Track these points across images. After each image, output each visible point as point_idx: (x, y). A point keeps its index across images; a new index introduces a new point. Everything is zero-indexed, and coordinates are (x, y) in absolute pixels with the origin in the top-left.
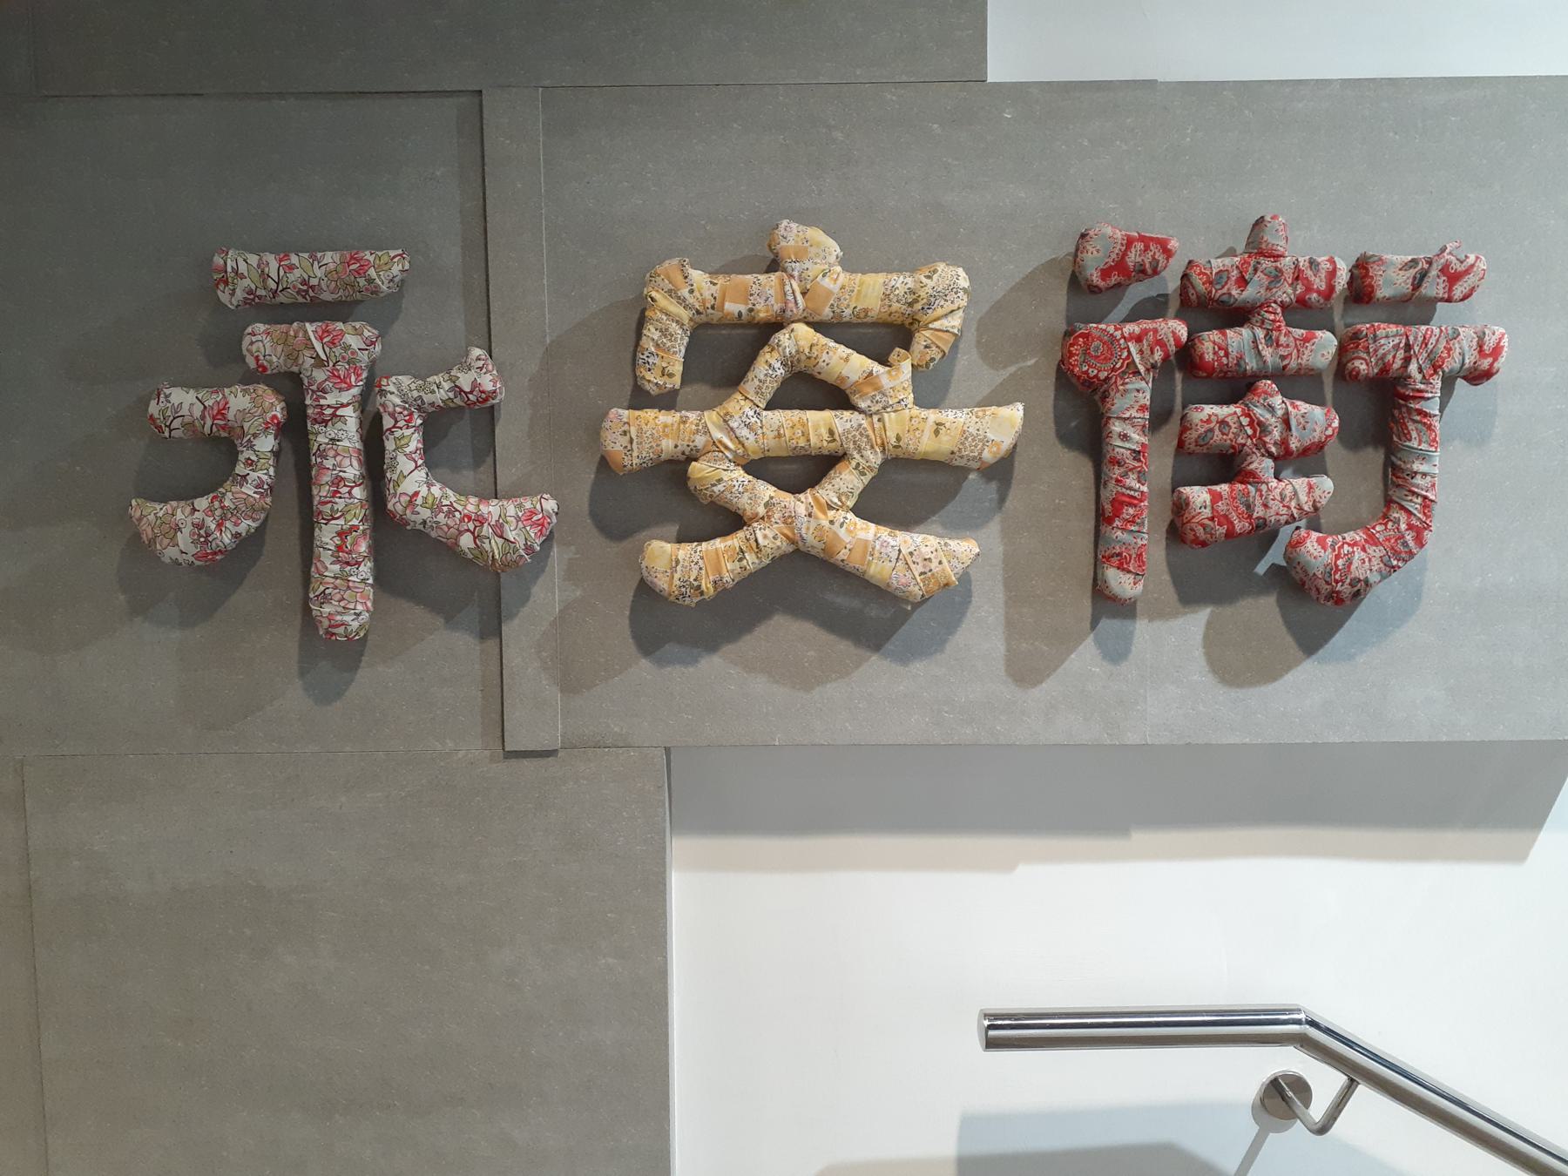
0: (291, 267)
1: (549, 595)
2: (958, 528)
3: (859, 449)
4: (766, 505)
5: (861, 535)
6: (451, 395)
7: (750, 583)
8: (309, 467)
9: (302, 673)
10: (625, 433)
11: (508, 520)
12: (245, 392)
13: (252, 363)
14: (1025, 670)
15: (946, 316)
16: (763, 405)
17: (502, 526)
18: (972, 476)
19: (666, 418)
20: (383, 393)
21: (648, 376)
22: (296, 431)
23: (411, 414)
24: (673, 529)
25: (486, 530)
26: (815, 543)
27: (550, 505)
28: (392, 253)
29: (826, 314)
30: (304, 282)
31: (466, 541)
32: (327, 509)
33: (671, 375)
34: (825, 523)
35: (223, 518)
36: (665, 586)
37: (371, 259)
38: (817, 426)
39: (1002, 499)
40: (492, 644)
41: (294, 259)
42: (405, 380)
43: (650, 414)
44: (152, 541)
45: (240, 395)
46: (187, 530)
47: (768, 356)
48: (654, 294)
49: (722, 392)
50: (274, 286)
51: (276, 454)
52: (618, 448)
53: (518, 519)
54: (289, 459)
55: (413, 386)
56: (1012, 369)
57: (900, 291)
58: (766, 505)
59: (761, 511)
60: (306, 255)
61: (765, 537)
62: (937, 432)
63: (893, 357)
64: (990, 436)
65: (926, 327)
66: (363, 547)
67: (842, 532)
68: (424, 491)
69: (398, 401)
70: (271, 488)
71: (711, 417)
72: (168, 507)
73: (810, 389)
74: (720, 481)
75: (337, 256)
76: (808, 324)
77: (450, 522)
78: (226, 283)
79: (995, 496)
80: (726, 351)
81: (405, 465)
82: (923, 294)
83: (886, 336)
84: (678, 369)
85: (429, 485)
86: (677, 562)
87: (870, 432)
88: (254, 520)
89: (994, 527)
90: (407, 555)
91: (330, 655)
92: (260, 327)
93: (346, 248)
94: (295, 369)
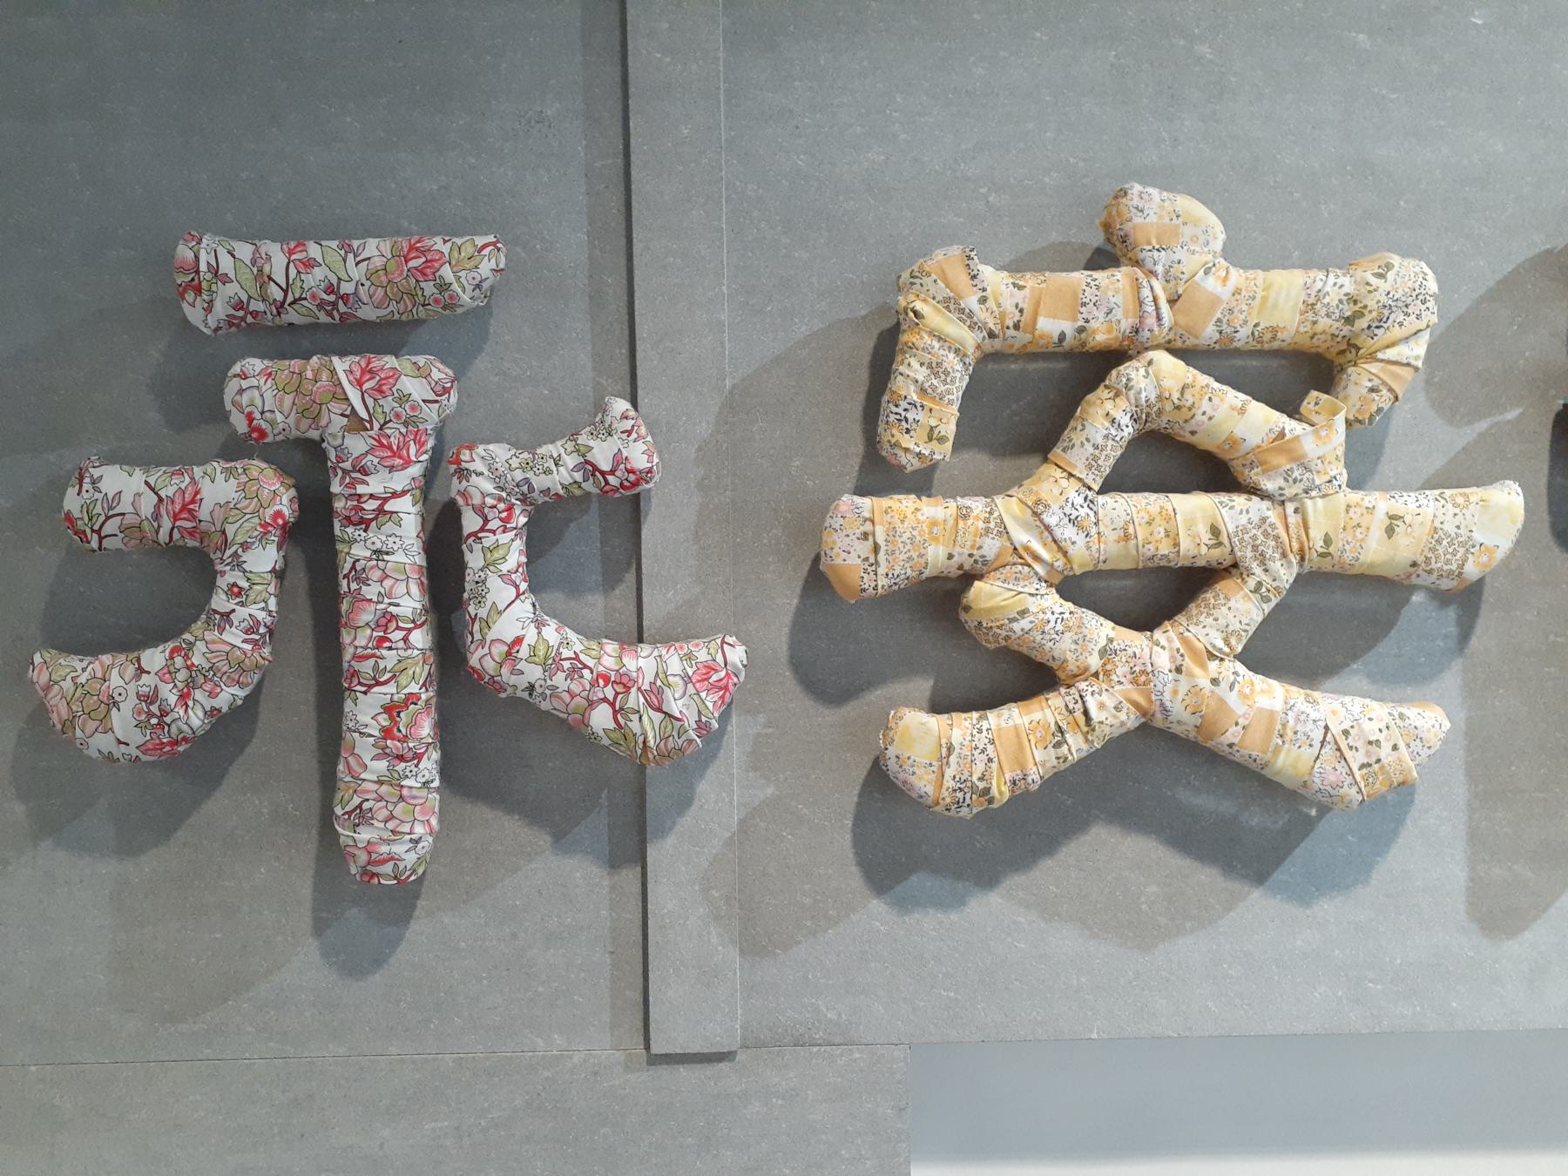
0: (310, 264)
1: (723, 796)
2: (1401, 680)
3: (1262, 560)
4: (1103, 652)
5: (1263, 702)
6: (578, 476)
7: (1062, 780)
8: (337, 597)
9: (319, 927)
10: (865, 536)
11: (670, 679)
12: (229, 473)
13: (240, 425)
14: (1497, 913)
15: (1406, 339)
16: (1096, 488)
17: (660, 692)
18: (1417, 598)
19: (934, 510)
20: (463, 474)
21: (906, 441)
22: (313, 535)
23: (510, 509)
24: (923, 686)
25: (635, 700)
26: (1185, 715)
27: (737, 655)
28: (480, 241)
29: (1208, 334)
30: (330, 289)
31: (601, 719)
32: (366, 667)
33: (942, 440)
34: (1204, 683)
35: (191, 684)
36: (930, 790)
37: (446, 249)
38: (1189, 520)
39: (1465, 636)
40: (630, 875)
41: (314, 251)
42: (501, 452)
43: (905, 503)
44: (69, 724)
45: (220, 478)
46: (129, 705)
47: (1109, 405)
48: (919, 306)
49: (1010, 465)
50: (279, 295)
51: (279, 575)
52: (853, 560)
53: (687, 679)
54: (299, 578)
55: (515, 463)
56: (1482, 426)
57: (1333, 297)
58: (1103, 652)
59: (1094, 662)
60: (334, 244)
61: (1102, 706)
62: (1390, 531)
63: (1307, 406)
64: (1478, 537)
65: (1372, 357)
66: (426, 729)
67: (1232, 699)
68: (531, 635)
69: (488, 487)
70: (271, 632)
71: (1009, 507)
72: (96, 666)
73: (1175, 458)
74: (1023, 613)
75: (386, 246)
76: (1175, 352)
77: (575, 687)
78: (198, 290)
79: (1453, 630)
80: (1032, 402)
81: (500, 592)
82: (1372, 304)
83: (1299, 372)
84: (949, 429)
85: (539, 625)
86: (950, 749)
87: (1281, 531)
88: (242, 686)
89: (1452, 679)
90: (491, 734)
91: (362, 905)
92: (255, 364)
93: (397, 232)
94: (314, 434)
